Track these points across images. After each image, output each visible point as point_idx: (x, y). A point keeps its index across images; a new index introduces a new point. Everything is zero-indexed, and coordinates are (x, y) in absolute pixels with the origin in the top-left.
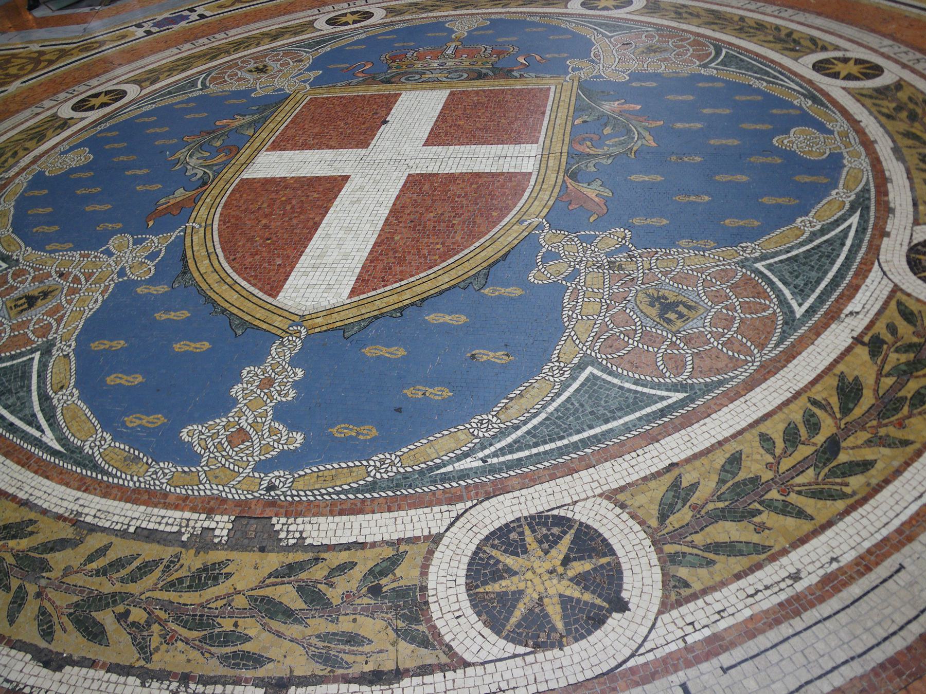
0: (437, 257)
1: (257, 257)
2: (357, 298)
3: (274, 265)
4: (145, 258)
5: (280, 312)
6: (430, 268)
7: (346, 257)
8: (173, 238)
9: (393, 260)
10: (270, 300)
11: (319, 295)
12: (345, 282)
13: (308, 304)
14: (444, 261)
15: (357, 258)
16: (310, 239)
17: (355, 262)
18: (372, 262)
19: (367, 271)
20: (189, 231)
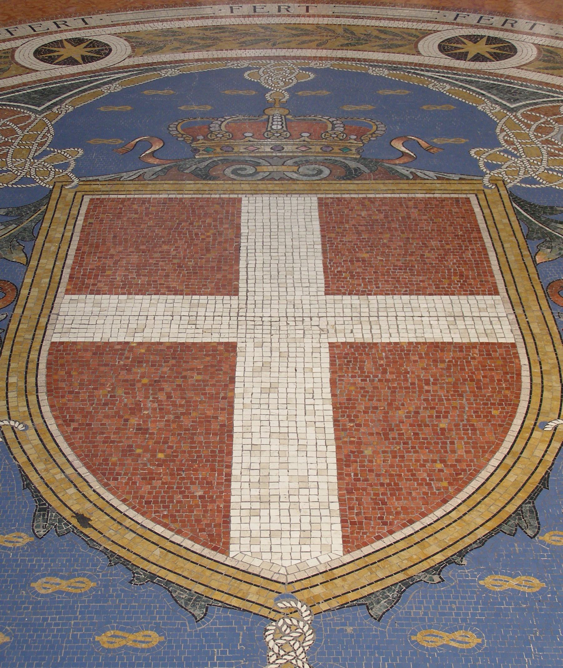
0: (445, 484)
1: (157, 483)
2: (357, 554)
3: (194, 497)
5: (247, 578)
6: (445, 501)
9: (382, 490)
10: (219, 557)
11: (297, 548)
12: (326, 527)
13: (287, 563)
14: (459, 490)
15: (323, 486)
16: (230, 453)
17: (323, 492)
18: (350, 492)
19: (351, 508)
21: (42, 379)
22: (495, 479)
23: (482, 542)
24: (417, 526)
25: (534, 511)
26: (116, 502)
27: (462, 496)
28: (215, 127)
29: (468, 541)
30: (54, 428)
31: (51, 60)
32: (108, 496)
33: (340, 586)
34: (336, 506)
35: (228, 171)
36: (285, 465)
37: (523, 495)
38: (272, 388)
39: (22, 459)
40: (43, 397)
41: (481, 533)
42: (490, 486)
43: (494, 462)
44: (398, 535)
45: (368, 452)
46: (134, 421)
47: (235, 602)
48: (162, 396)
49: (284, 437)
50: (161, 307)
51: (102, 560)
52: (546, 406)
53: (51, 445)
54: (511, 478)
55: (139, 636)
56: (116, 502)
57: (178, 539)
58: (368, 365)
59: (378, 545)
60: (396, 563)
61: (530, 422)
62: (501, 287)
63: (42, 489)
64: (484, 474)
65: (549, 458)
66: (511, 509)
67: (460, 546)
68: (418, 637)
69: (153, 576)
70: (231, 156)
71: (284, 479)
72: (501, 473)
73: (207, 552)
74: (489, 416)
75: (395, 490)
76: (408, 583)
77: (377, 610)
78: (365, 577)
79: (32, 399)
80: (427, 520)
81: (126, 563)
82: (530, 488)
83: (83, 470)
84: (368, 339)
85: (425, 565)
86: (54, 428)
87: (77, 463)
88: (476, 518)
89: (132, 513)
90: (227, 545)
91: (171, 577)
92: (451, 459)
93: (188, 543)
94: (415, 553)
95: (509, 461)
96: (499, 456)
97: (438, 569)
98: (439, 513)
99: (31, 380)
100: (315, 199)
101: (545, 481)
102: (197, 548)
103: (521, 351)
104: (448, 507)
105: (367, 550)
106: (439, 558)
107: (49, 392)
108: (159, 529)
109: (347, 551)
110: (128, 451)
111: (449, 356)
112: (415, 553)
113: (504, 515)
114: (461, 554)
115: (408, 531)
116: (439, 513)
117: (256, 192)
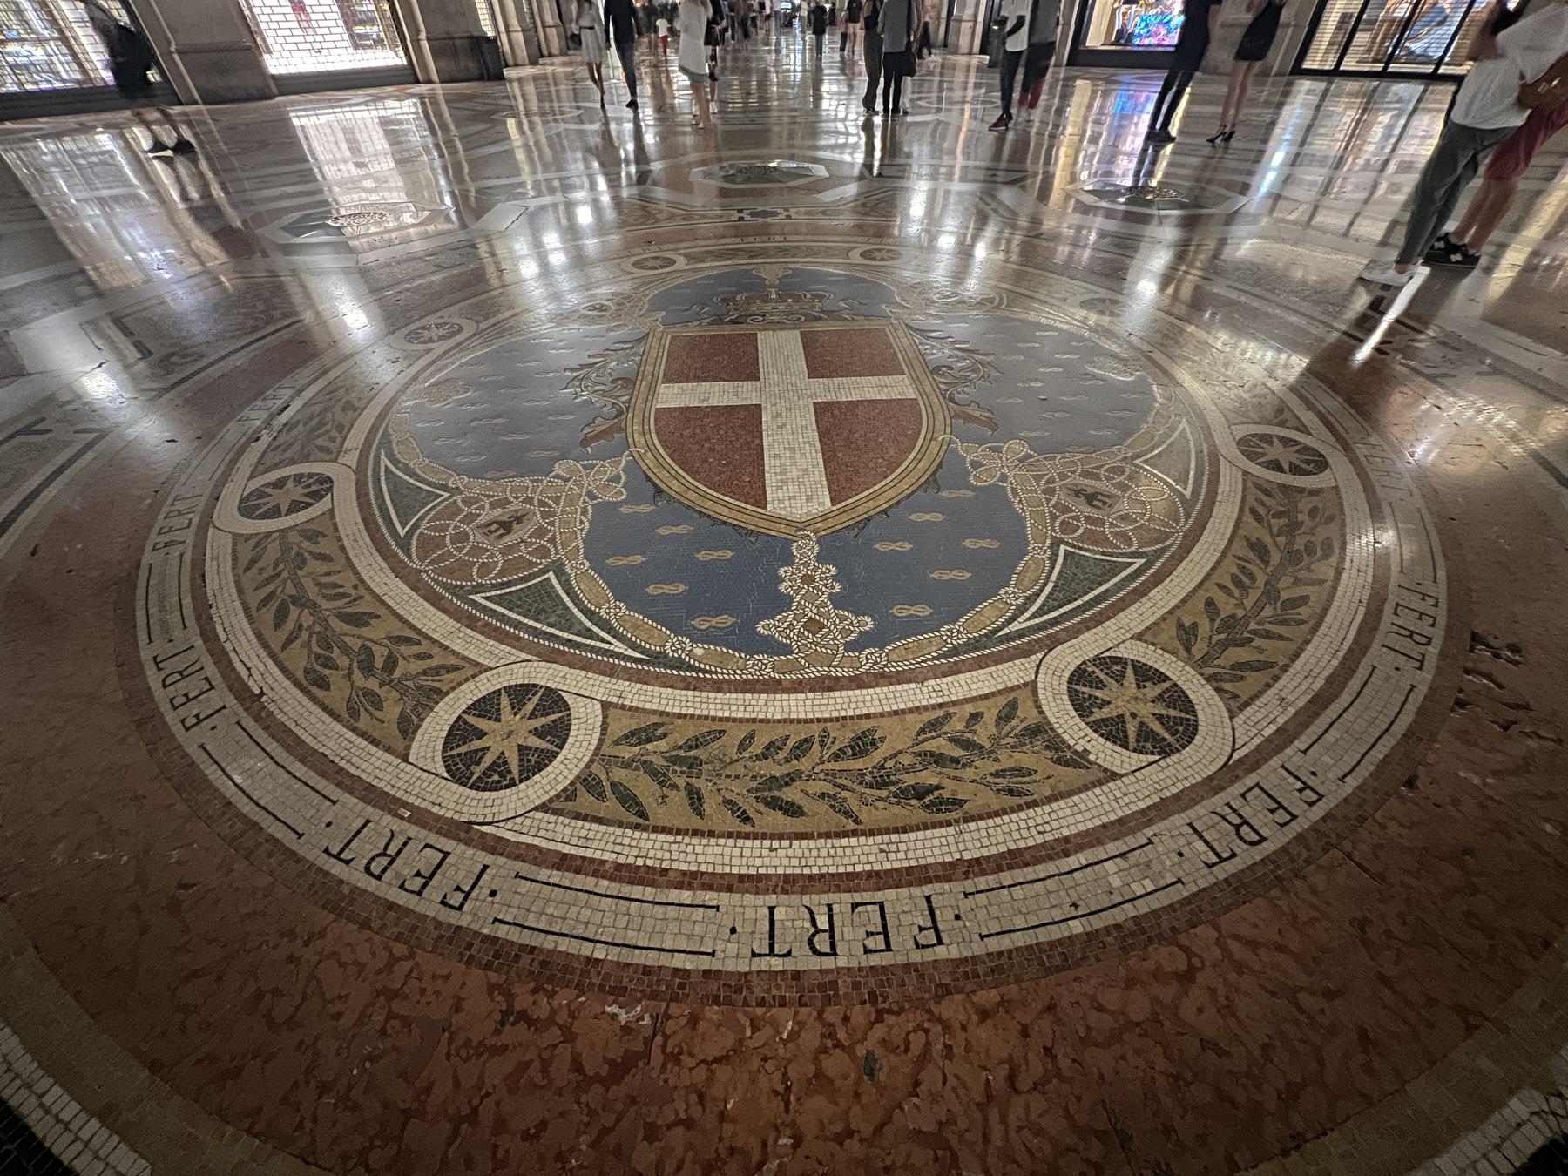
2: (839, 506)
4: (608, 480)
7: (806, 471)
8: (624, 462)
20: (636, 455)
21: (652, 427)
22: (912, 465)
23: (908, 496)
24: (871, 490)
25: (935, 480)
26: (701, 486)
27: (895, 475)
28: (738, 298)
29: (900, 497)
30: (661, 451)
31: (643, 268)
32: (696, 484)
33: (831, 522)
34: (825, 483)
35: (749, 320)
36: (794, 464)
37: (929, 473)
38: (784, 425)
39: (645, 468)
40: (654, 435)
41: (908, 492)
42: (909, 469)
43: (911, 457)
44: (861, 496)
45: (840, 455)
46: (706, 445)
47: (773, 533)
48: (722, 432)
49: (792, 450)
50: (717, 389)
51: (696, 515)
52: (937, 428)
53: (661, 460)
54: (921, 465)
55: (721, 553)
56: (701, 486)
57: (737, 503)
58: (836, 412)
59: (851, 501)
60: (861, 509)
61: (929, 436)
62: (906, 371)
63: (657, 481)
64: (906, 463)
65: (941, 454)
66: (923, 480)
67: (896, 500)
68: (878, 546)
69: (725, 523)
70: (749, 312)
71: (795, 470)
72: (915, 462)
73: (754, 509)
74: (906, 435)
75: (857, 473)
76: (868, 519)
77: (853, 533)
78: (844, 517)
79: (648, 437)
80: (876, 488)
81: (709, 516)
82: (931, 470)
83: (680, 471)
84: (834, 399)
85: (878, 510)
86: (661, 451)
87: (676, 468)
88: (903, 485)
89: (710, 491)
90: (766, 505)
91: (735, 522)
92: (887, 457)
93: (743, 505)
94: (871, 504)
95: (919, 456)
96: (913, 454)
97: (885, 512)
98: (883, 483)
99: (646, 427)
100: (797, 332)
101: (940, 466)
102: (749, 507)
103: (921, 402)
104: (888, 480)
105: (844, 504)
106: (885, 506)
107: (657, 433)
108: (726, 499)
109: (833, 505)
110: (705, 461)
111: (879, 406)
112: (871, 504)
113: (919, 483)
114: (898, 503)
115: (867, 493)
116: (883, 483)
117: (764, 330)
